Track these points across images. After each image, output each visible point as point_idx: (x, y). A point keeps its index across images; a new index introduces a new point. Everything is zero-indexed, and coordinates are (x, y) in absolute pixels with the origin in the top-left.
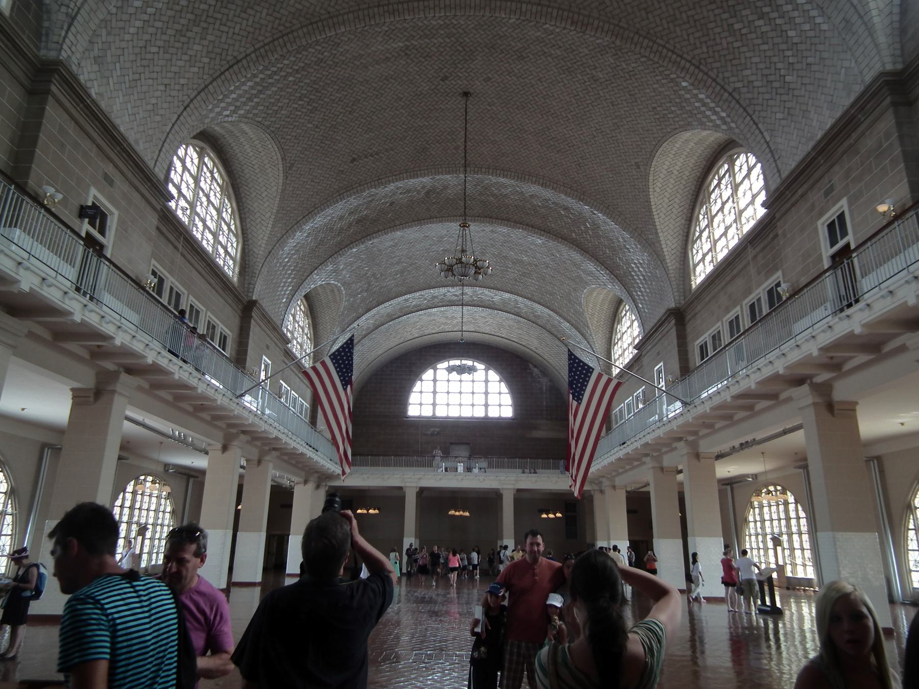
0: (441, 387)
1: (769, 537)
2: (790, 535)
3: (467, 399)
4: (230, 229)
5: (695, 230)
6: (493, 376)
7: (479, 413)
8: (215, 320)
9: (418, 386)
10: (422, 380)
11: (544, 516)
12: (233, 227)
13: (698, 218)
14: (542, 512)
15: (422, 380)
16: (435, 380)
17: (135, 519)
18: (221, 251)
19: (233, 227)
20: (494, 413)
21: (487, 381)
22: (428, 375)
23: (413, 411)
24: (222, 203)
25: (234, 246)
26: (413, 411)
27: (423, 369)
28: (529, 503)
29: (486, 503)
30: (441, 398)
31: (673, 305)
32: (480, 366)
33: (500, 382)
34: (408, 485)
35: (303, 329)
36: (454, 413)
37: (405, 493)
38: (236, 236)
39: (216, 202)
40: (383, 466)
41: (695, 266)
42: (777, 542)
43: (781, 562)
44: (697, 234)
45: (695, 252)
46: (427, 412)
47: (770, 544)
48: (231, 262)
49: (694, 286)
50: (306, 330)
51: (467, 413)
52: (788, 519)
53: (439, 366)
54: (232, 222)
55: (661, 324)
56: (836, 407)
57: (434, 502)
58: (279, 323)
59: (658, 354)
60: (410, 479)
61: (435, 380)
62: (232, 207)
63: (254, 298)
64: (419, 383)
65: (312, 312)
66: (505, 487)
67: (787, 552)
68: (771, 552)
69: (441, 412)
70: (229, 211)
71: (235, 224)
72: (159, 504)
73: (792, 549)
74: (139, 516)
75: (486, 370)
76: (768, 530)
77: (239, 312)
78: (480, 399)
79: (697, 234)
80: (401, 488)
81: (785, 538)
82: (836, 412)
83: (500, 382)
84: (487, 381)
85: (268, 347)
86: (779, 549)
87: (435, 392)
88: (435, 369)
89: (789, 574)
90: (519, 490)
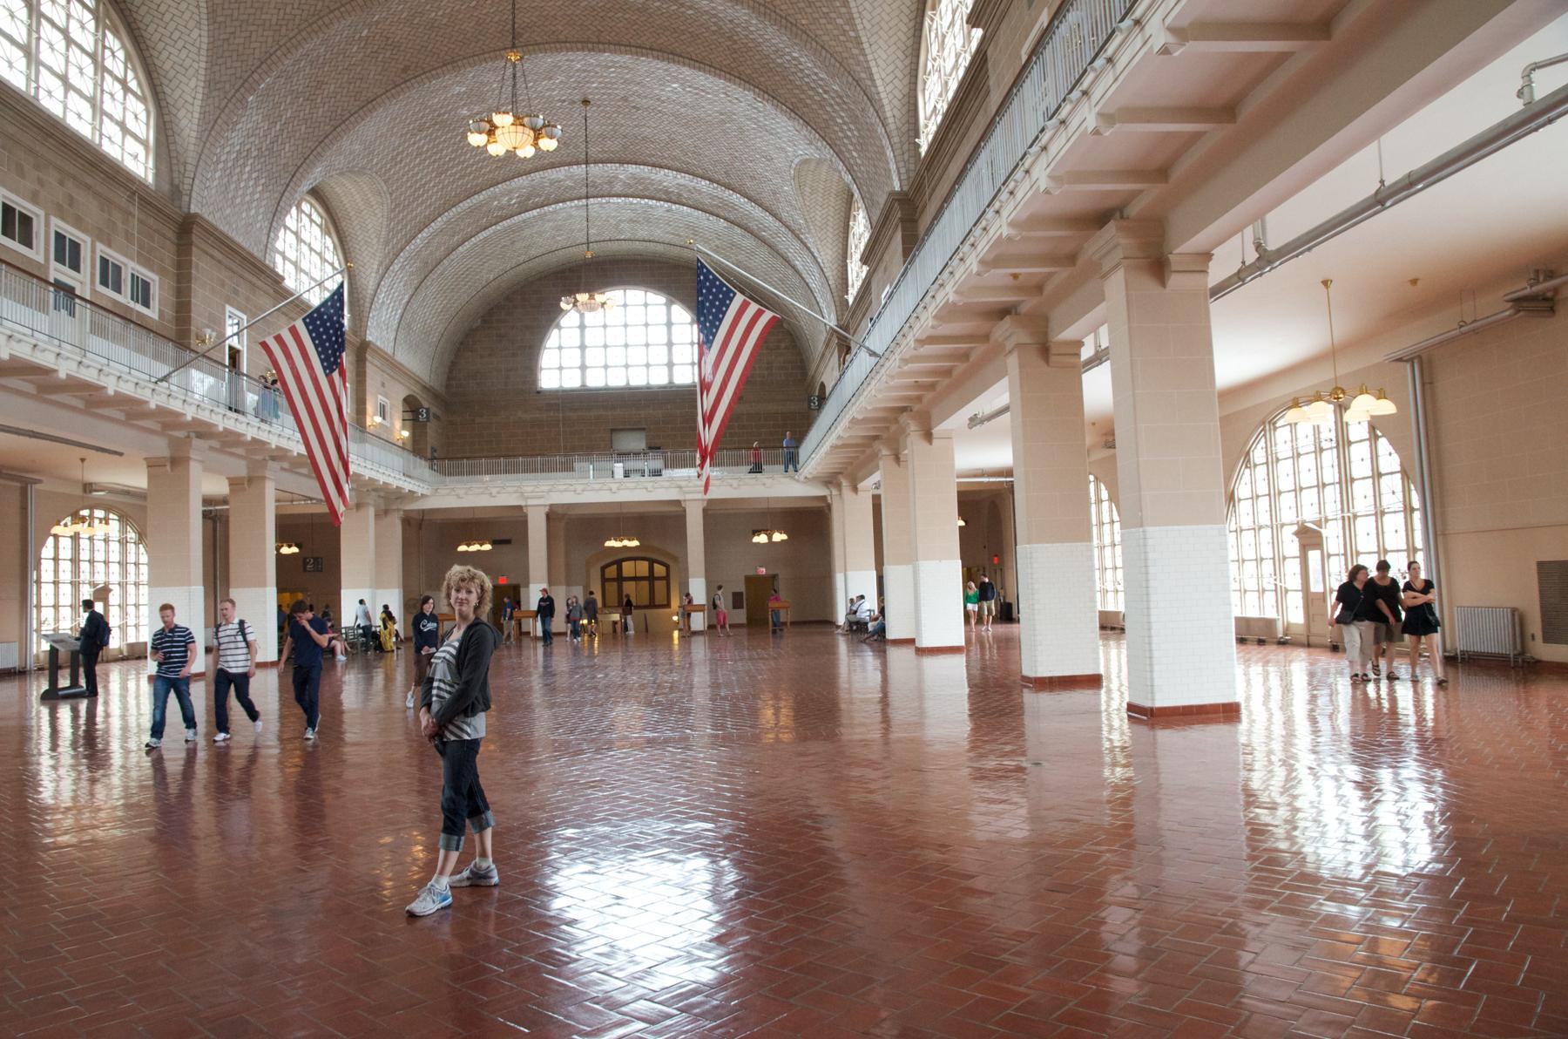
0: (592, 337)
3: (636, 356)
4: (126, 89)
7: (659, 378)
8: (115, 256)
9: (553, 338)
10: (559, 328)
11: (762, 539)
12: (133, 85)
14: (757, 532)
15: (559, 328)
17: (85, 576)
18: (110, 128)
19: (133, 85)
21: (669, 324)
23: (548, 380)
24: (100, 42)
25: (139, 116)
26: (548, 380)
28: (727, 521)
29: (659, 525)
30: (594, 356)
31: (897, 188)
32: (657, 299)
34: (530, 502)
35: (320, 254)
36: (617, 380)
37: (526, 516)
38: (142, 99)
39: (88, 41)
40: (469, 473)
46: (571, 381)
48: (140, 150)
50: (329, 256)
51: (638, 379)
52: (75, 561)
54: (130, 75)
56: (1053, 351)
57: (577, 529)
58: (256, 252)
60: (537, 493)
62: (123, 47)
63: (194, 209)
64: (554, 333)
65: (335, 224)
66: (688, 497)
69: (595, 380)
70: (121, 55)
71: (136, 77)
72: (124, 552)
74: (92, 573)
75: (669, 305)
77: (171, 235)
78: (660, 355)
80: (520, 508)
82: (1053, 359)
84: (669, 324)
85: (236, 292)
87: (583, 347)
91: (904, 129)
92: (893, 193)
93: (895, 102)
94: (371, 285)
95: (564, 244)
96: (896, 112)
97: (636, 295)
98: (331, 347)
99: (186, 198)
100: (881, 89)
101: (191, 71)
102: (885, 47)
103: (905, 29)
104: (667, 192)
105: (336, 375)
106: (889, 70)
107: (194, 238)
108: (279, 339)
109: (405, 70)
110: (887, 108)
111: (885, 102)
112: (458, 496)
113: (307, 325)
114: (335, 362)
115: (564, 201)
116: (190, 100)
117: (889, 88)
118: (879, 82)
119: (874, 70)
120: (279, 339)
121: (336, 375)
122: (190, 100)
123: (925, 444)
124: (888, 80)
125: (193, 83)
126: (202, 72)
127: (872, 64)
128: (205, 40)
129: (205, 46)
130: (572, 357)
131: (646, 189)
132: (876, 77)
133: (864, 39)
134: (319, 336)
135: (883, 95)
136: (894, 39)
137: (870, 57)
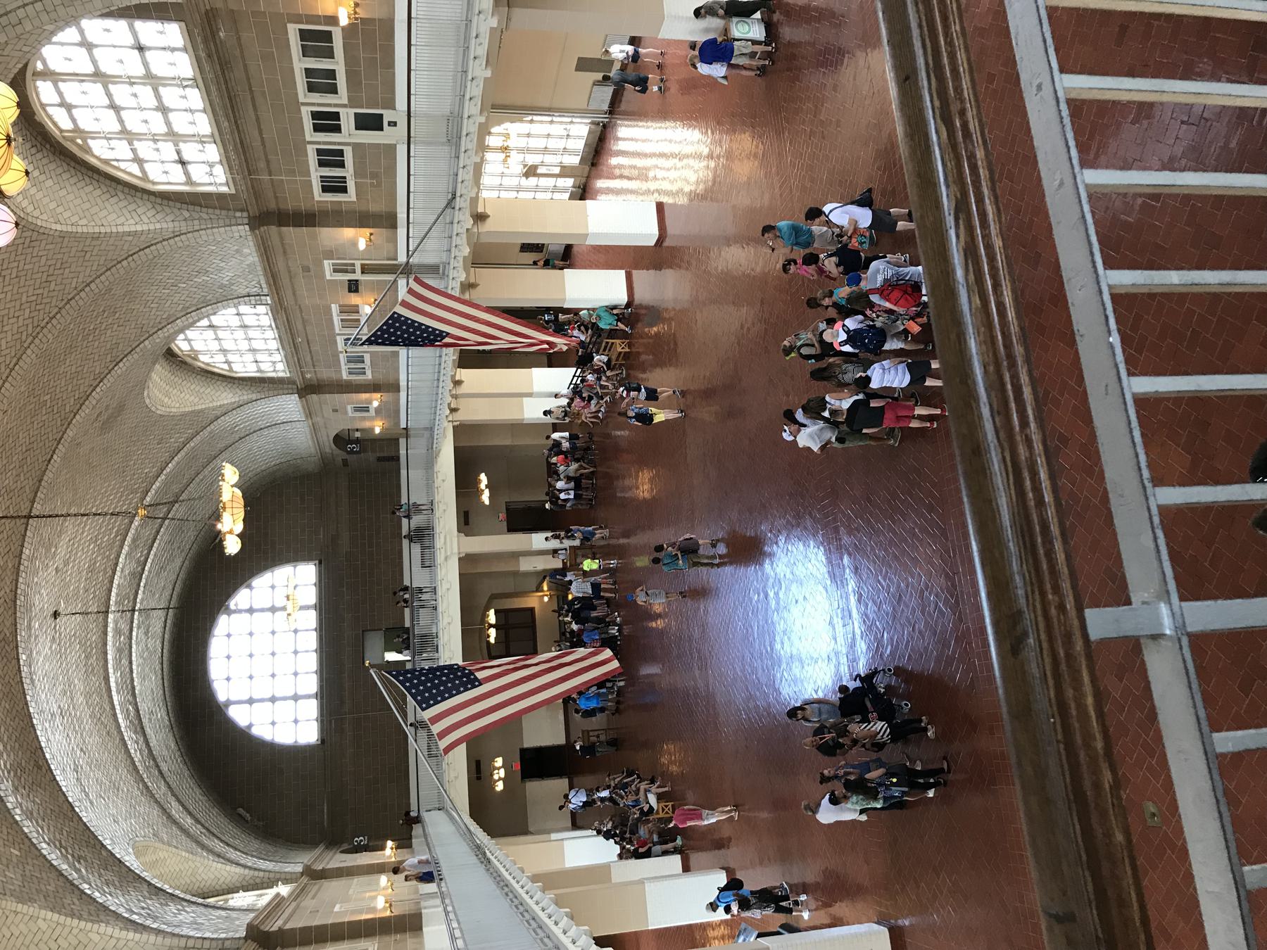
0: (262, 689)
1: (525, 182)
2: (529, 150)
5: (124, 171)
6: (241, 598)
7: (310, 619)
9: (262, 731)
10: (250, 726)
13: (106, 162)
15: (250, 726)
16: (251, 701)
20: (310, 595)
22: (239, 715)
27: (230, 724)
30: (285, 687)
32: (223, 624)
33: (249, 587)
36: (310, 662)
41: (189, 181)
42: (531, 172)
43: (557, 170)
44: (134, 168)
45: (163, 179)
46: (311, 709)
47: (533, 181)
49: (224, 189)
51: (310, 641)
53: (221, 697)
55: (266, 252)
59: (306, 269)
61: (251, 701)
64: (256, 731)
66: (456, 550)
67: (549, 159)
68: (544, 182)
69: (311, 684)
73: (545, 150)
75: (229, 612)
76: (514, 182)
79: (134, 168)
81: (532, 159)
83: (249, 587)
84: (251, 611)
86: (539, 171)
88: (228, 703)
89: (575, 160)
90: (459, 531)
91: (186, 214)
92: (252, 229)
93: (159, 217)
94: (239, 870)
95: (164, 714)
96: (169, 218)
97: (218, 648)
98: (452, 681)
99: (227, 944)
100: (145, 227)
101: (81, 937)
102: (104, 213)
103: (90, 188)
104: (132, 574)
105: (480, 675)
106: (128, 216)
107: (275, 928)
108: (442, 735)
109: (39, 768)
110: (165, 225)
111: (158, 226)
112: (456, 778)
113: (429, 706)
114: (468, 676)
115: (133, 688)
116: (113, 941)
117: (146, 220)
118: (139, 228)
119: (127, 229)
120: (442, 735)
121: (480, 675)
122: (113, 941)
123: (489, 221)
124: (137, 219)
125: (96, 938)
126: (83, 924)
127: (120, 229)
128: (50, 914)
129: (56, 916)
130: (285, 710)
131: (127, 597)
132: (133, 229)
133: (97, 230)
134: (441, 694)
135: (152, 227)
136: (98, 200)
137: (114, 230)
